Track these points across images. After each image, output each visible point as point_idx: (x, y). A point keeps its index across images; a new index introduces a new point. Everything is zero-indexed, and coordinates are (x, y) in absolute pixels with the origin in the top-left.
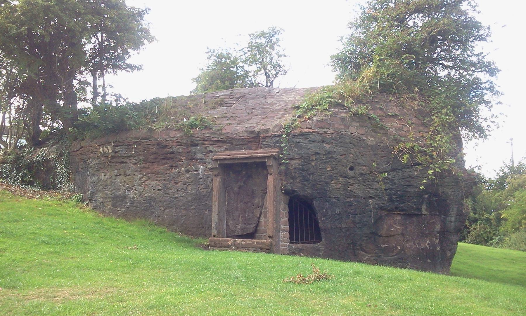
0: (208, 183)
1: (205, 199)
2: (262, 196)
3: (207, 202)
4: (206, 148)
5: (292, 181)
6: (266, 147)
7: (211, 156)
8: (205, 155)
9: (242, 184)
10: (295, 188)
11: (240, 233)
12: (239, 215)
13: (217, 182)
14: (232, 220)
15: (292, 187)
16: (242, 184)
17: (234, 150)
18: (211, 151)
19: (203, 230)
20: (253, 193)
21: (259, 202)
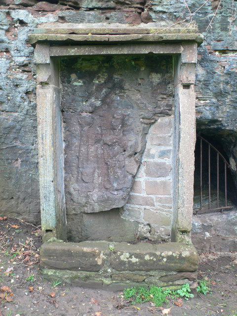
0: (18, 99)
1: (12, 135)
2: (144, 129)
3: (18, 144)
4: (8, 14)
5: (214, 100)
6: (162, 19)
7: (23, 34)
8: (7, 31)
9: (98, 103)
10: (220, 116)
11: (97, 208)
12: (94, 171)
13: (47, 100)
14: (77, 181)
15: (213, 114)
16: (98, 103)
17: (82, 21)
18: (22, 23)
19: (13, 202)
20: (123, 123)
21: (136, 143)
